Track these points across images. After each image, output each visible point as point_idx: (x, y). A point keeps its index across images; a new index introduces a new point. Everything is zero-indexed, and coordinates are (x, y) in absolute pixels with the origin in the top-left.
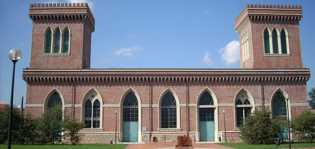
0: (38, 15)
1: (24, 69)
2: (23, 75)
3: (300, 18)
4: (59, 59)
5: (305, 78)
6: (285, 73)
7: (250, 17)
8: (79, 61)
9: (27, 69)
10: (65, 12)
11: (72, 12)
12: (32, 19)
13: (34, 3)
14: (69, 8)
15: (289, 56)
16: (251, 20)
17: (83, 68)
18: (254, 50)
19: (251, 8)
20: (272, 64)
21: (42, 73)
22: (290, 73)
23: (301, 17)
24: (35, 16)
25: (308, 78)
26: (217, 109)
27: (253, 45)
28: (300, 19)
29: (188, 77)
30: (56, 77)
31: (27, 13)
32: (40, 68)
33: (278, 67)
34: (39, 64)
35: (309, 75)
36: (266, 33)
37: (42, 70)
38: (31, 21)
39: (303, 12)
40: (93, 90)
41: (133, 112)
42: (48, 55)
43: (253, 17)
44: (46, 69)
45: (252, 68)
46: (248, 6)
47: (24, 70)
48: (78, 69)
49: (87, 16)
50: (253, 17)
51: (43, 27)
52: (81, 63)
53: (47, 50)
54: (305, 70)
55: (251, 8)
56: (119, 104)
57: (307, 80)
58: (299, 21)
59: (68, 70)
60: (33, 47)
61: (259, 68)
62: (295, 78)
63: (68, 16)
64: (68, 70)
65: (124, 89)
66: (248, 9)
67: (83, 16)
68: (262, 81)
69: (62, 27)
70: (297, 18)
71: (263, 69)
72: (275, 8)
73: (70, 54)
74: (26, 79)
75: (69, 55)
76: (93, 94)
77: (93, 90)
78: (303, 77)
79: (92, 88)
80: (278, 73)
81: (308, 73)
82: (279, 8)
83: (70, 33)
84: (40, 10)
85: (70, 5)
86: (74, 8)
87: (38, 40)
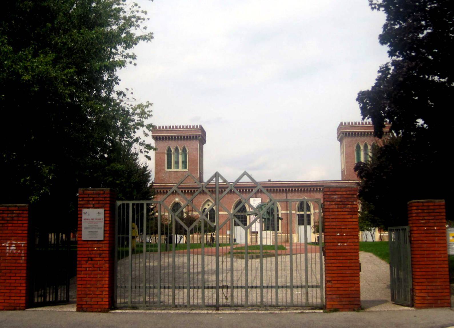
7: (343, 133)
10: (182, 133)
11: (189, 133)
16: (344, 136)
18: (346, 163)
21: (166, 187)
26: (313, 214)
34: (163, 179)
36: (358, 147)
41: (242, 218)
42: (169, 171)
43: (346, 134)
44: (169, 183)
46: (341, 123)
48: (195, 183)
49: (202, 137)
51: (164, 145)
61: (351, 179)
63: (186, 136)
67: (198, 137)
69: (180, 145)
73: (188, 170)
75: (187, 171)
83: (187, 152)
84: (161, 132)
85: (187, 127)
87: (160, 158)
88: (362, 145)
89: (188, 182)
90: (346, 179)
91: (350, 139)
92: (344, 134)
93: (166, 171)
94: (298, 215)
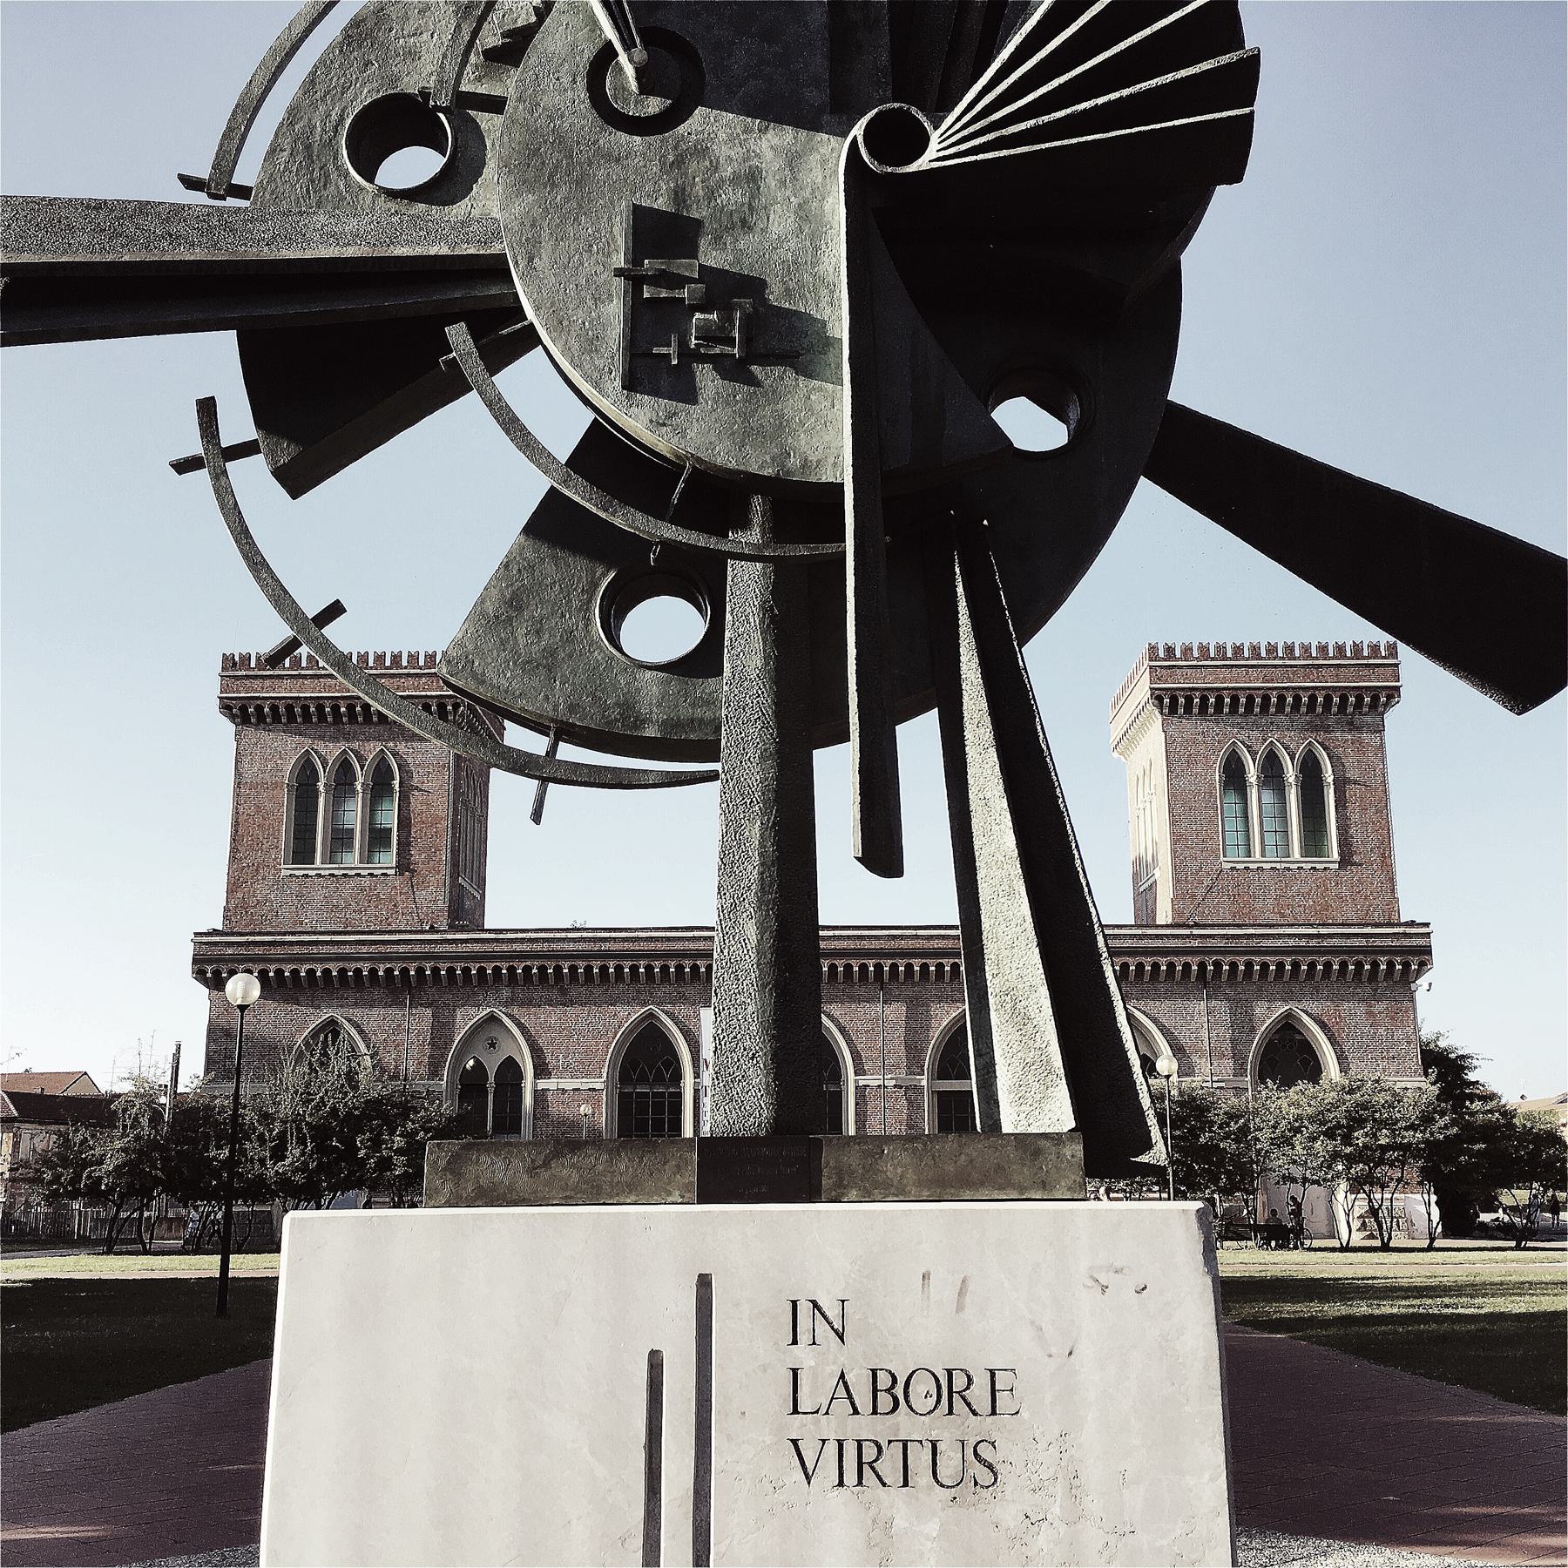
0: (259, 702)
1: (196, 934)
2: (195, 961)
3: (1390, 697)
4: (348, 888)
5: (1406, 965)
6: (1313, 943)
7: (1160, 699)
8: (433, 896)
9: (215, 932)
12: (232, 718)
13: (237, 650)
14: (392, 671)
15: (1337, 866)
16: (1166, 711)
17: (453, 928)
19: (1163, 659)
20: (1259, 905)
22: (1336, 942)
23: (1393, 693)
24: (244, 709)
25: (1422, 964)
27: (1173, 823)
28: (1387, 705)
29: (890, 962)
30: (341, 964)
31: (210, 688)
32: (269, 929)
33: (1283, 916)
35: (1427, 951)
37: (278, 938)
38: (230, 728)
39: (1402, 671)
40: (492, 1019)
43: (1174, 700)
44: (293, 934)
45: (1170, 921)
46: (1153, 649)
47: (199, 939)
48: (433, 930)
50: (1174, 700)
52: (442, 904)
53: (302, 853)
54: (1408, 930)
55: (1163, 659)
56: (600, 1077)
57: (1419, 973)
58: (1383, 714)
59: (386, 937)
60: (235, 839)
62: (1359, 965)
64: (386, 937)
65: (628, 1015)
66: (1151, 667)
67: (450, 708)
68: (1209, 977)
70: (1375, 699)
71: (1212, 926)
72: (1275, 659)
74: (209, 975)
76: (495, 1032)
77: (492, 1019)
78: (1399, 959)
79: (489, 1010)
80: (1279, 943)
81: (1421, 942)
82: (1295, 659)
84: (268, 683)
85: (396, 658)
86: (412, 671)
88: (1253, 754)
89: (393, 927)
90: (1181, 921)
91: (1190, 727)
92: (1167, 701)
93: (284, 873)
94: (942, 1095)
